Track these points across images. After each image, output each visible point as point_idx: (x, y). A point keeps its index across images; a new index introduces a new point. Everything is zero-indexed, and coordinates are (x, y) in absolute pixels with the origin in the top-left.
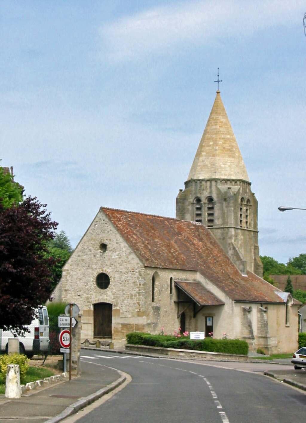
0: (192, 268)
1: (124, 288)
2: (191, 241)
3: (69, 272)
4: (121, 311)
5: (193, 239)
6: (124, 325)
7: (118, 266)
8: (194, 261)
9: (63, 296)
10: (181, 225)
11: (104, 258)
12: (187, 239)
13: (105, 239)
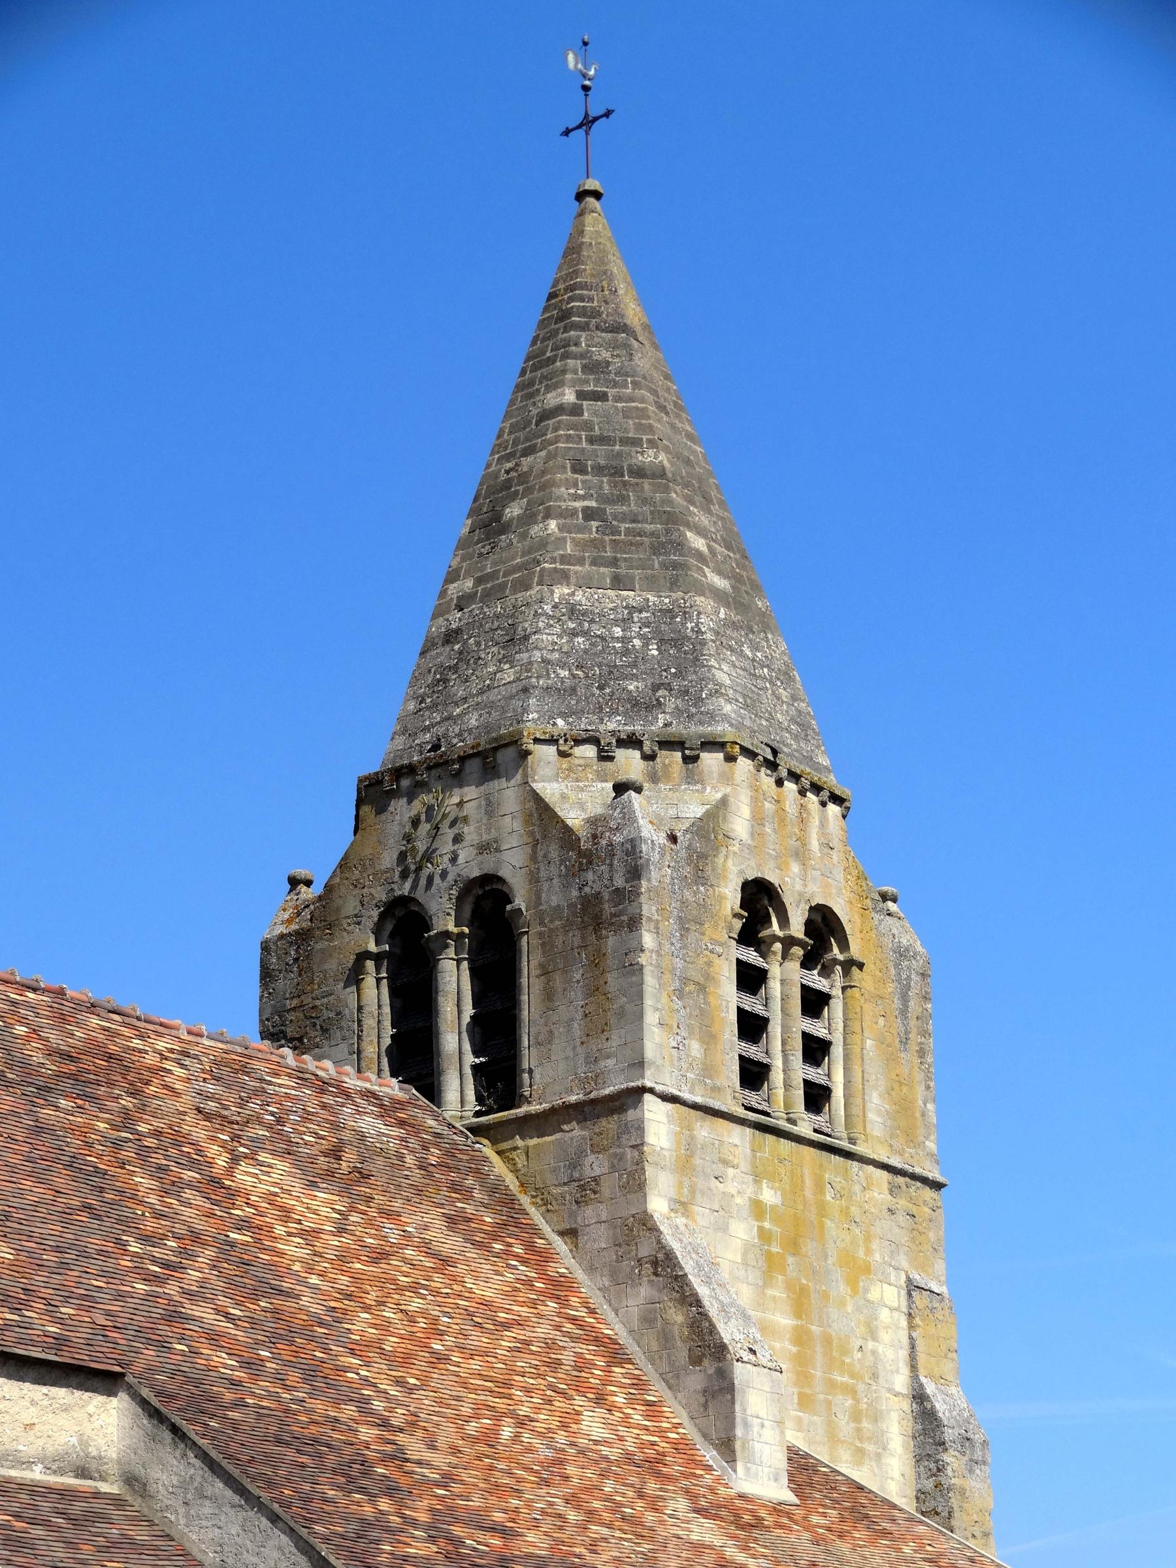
0: (60, 1342)
2: (198, 1162)
5: (235, 1159)
8: (120, 1296)
10: (137, 1043)
12: (150, 1142)
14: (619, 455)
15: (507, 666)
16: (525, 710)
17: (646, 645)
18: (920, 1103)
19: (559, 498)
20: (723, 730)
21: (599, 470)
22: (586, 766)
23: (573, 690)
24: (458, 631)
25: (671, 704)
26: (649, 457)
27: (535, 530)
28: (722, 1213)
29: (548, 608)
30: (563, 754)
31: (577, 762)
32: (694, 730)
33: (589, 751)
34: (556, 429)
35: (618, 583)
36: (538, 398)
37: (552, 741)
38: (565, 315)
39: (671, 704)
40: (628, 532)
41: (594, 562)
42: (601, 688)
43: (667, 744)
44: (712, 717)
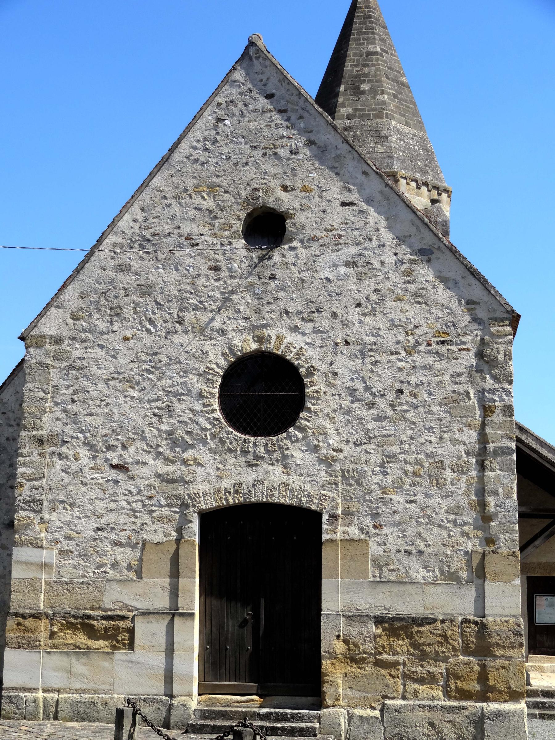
1: (391, 429)
3: (65, 347)
4: (375, 549)
6: (398, 624)
7: (354, 315)
9: (21, 470)
11: (273, 277)
13: (274, 184)
14: (396, 76)
15: (379, 146)
16: (393, 164)
17: (419, 149)
19: (385, 87)
20: (445, 185)
21: (393, 80)
22: (413, 189)
23: (404, 161)
24: (350, 127)
25: (431, 173)
26: (404, 79)
27: (378, 97)
29: (392, 127)
30: (408, 184)
31: (412, 188)
32: (439, 184)
33: (414, 184)
34: (377, 60)
35: (407, 124)
36: (364, 46)
37: (405, 178)
38: (369, 17)
39: (431, 173)
40: (406, 106)
41: (400, 114)
42: (411, 161)
43: (436, 188)
44: (441, 180)
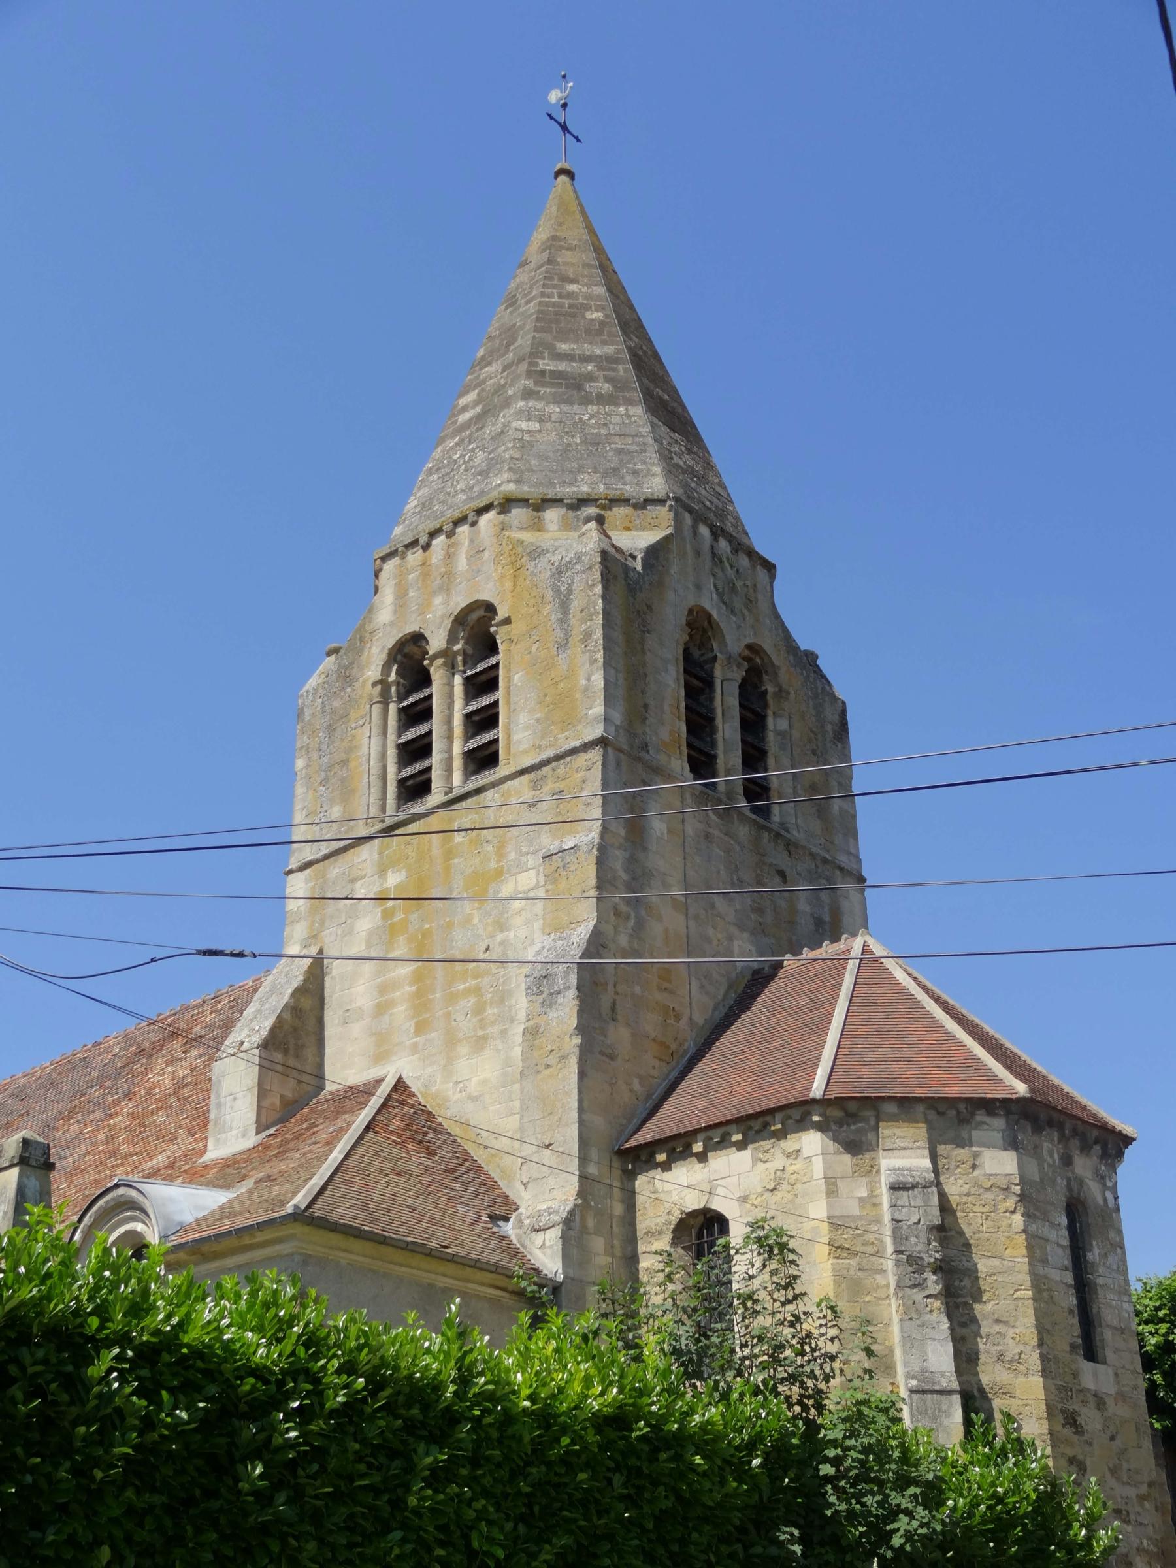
18: (583, 682)
28: (349, 921)
